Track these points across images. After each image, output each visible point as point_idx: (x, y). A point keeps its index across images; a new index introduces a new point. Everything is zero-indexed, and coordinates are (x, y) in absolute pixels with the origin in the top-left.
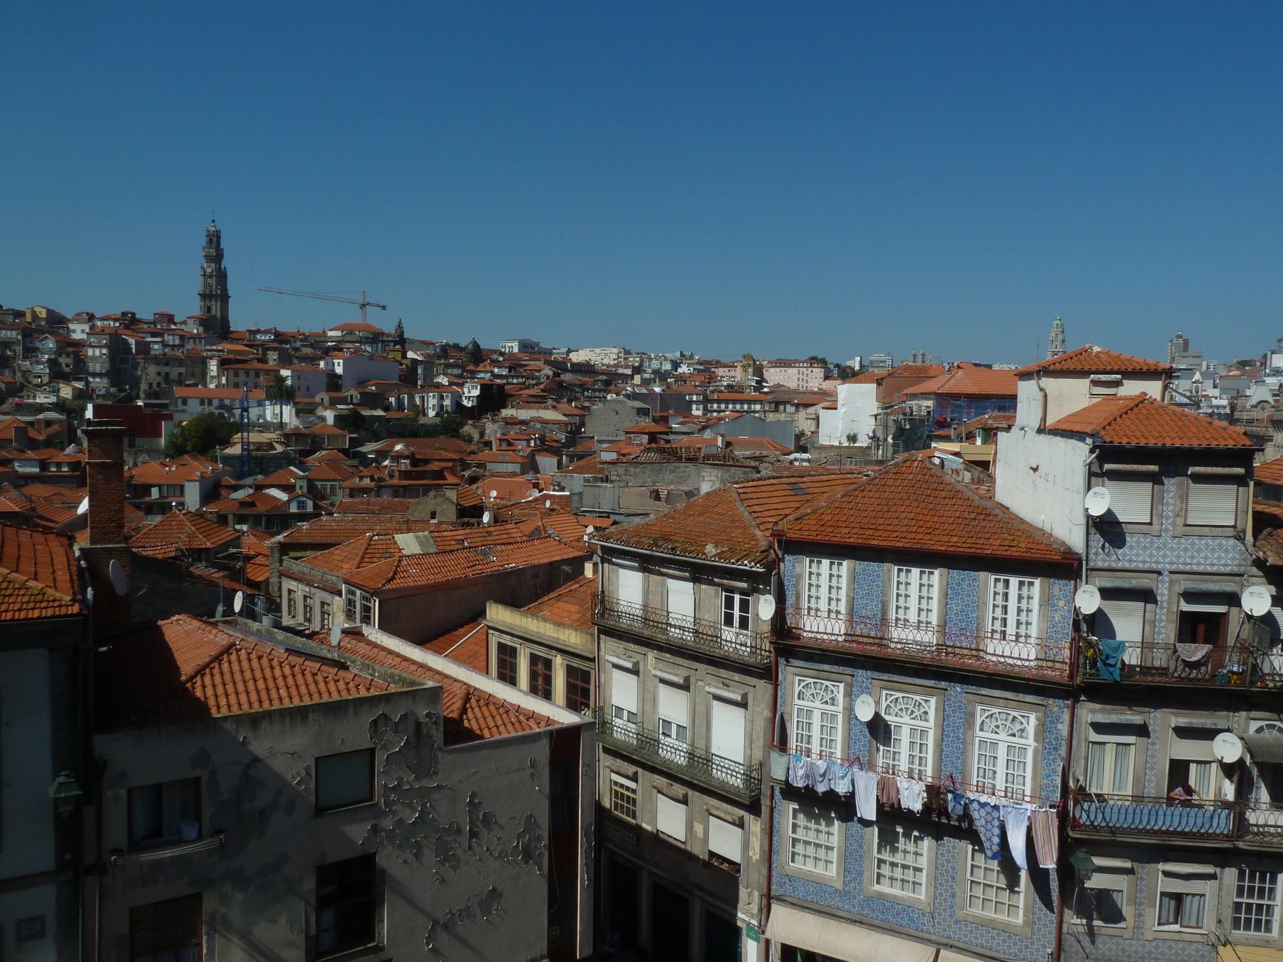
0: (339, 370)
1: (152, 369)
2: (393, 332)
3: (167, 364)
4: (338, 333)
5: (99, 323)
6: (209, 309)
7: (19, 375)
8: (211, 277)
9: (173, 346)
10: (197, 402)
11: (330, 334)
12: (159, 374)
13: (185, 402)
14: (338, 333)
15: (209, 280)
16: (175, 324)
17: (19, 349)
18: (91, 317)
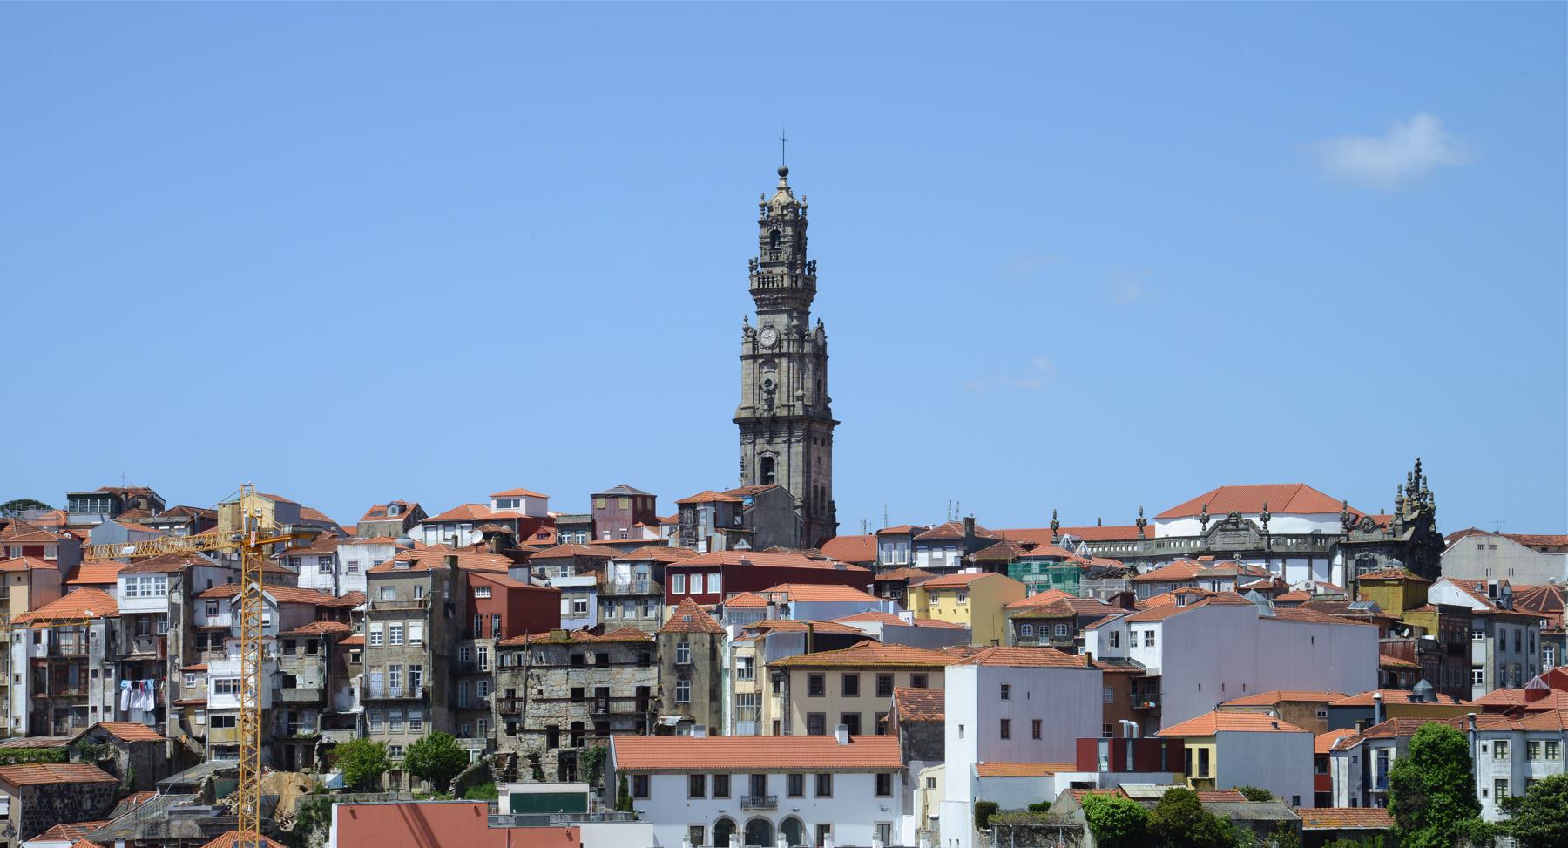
0: (1149, 659)
1: (559, 682)
2: (1391, 510)
3: (603, 661)
4: (1192, 527)
5: (433, 537)
6: (768, 464)
7: (172, 718)
8: (770, 360)
9: (632, 599)
10: (683, 782)
11: (1161, 530)
12: (577, 695)
13: (642, 789)
14: (1192, 527)
15: (768, 374)
16: (654, 522)
17: (175, 636)
18: (415, 517)
